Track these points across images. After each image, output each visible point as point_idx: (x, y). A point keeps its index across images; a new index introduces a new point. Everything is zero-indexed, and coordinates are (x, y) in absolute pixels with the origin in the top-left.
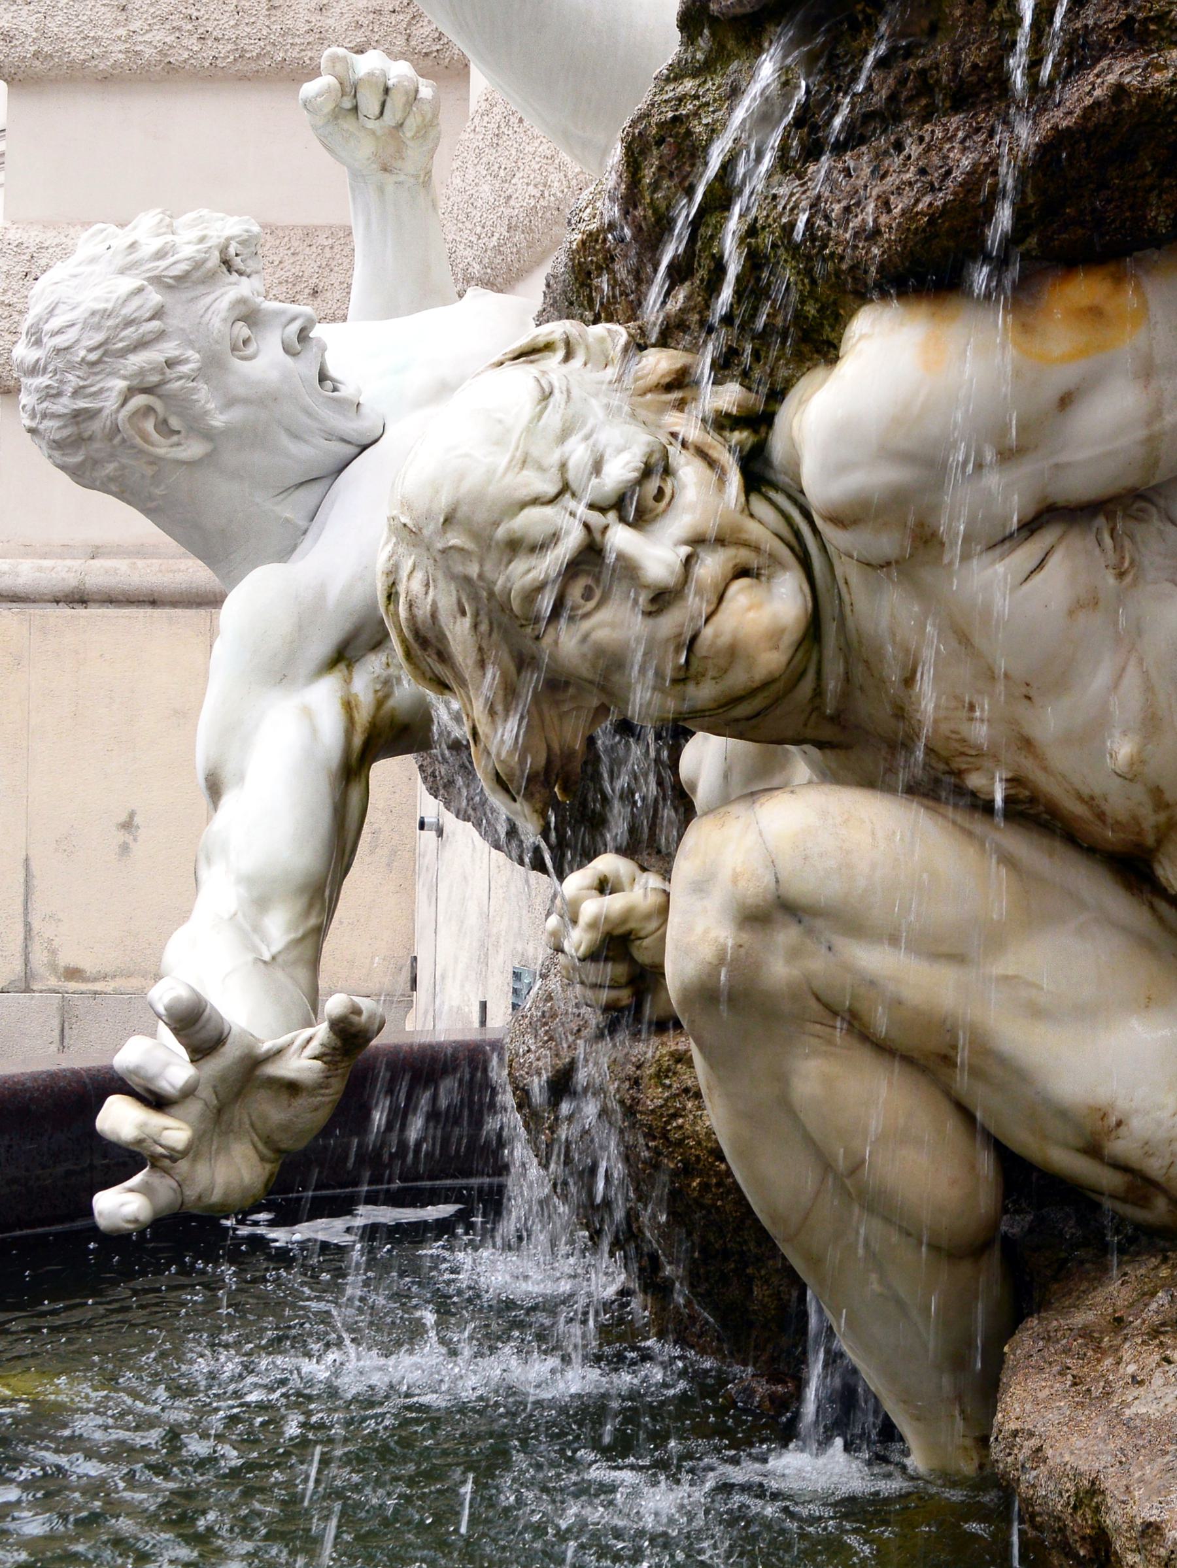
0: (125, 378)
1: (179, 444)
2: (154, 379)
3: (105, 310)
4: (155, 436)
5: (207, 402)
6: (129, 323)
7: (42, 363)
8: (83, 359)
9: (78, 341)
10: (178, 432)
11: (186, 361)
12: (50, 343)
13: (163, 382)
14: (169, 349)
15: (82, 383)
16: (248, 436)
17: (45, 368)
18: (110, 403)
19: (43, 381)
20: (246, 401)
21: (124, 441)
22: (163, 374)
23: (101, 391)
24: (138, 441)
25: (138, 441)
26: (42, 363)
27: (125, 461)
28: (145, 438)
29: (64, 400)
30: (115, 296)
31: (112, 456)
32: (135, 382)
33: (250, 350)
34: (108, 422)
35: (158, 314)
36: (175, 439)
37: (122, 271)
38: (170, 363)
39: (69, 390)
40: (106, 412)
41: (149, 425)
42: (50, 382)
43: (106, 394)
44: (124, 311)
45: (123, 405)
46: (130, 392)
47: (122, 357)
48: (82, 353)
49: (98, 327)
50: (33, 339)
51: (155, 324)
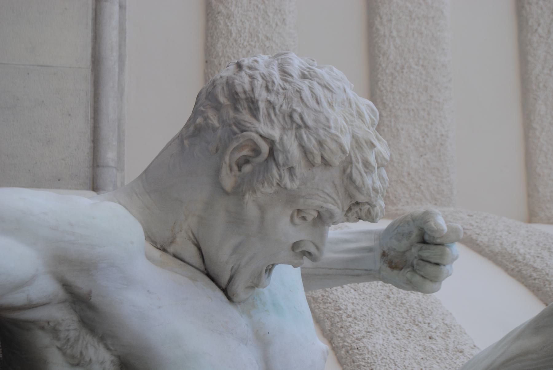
0: (281, 139)
1: (231, 170)
2: (281, 159)
3: (329, 127)
4: (238, 155)
5: (262, 193)
6: (321, 143)
7: (290, 79)
8: (294, 110)
9: (307, 106)
10: (240, 170)
11: (292, 180)
12: (304, 85)
13: (277, 165)
14: (301, 170)
15: (277, 108)
16: (237, 220)
17: (286, 81)
18: (264, 128)
19: (277, 79)
20: (262, 219)
21: (235, 134)
22: (284, 165)
23: (272, 122)
24: (235, 144)
25: (235, 144)
26: (290, 79)
27: (219, 131)
28: (237, 149)
29: (264, 94)
30: (339, 135)
31: (223, 122)
32: (278, 146)
33: (297, 220)
34: (249, 125)
35: (326, 163)
36: (235, 168)
37: (355, 138)
38: (291, 170)
39: (272, 98)
40: (257, 125)
41: (245, 152)
42: (277, 84)
43: (269, 124)
44: (329, 140)
45: (261, 136)
46: (271, 143)
47: (296, 136)
48: (299, 110)
49: (316, 121)
50: (306, 73)
51: (318, 160)
